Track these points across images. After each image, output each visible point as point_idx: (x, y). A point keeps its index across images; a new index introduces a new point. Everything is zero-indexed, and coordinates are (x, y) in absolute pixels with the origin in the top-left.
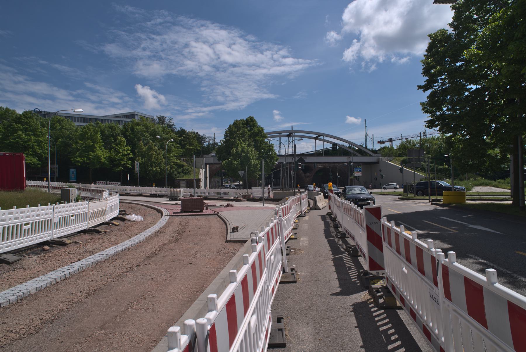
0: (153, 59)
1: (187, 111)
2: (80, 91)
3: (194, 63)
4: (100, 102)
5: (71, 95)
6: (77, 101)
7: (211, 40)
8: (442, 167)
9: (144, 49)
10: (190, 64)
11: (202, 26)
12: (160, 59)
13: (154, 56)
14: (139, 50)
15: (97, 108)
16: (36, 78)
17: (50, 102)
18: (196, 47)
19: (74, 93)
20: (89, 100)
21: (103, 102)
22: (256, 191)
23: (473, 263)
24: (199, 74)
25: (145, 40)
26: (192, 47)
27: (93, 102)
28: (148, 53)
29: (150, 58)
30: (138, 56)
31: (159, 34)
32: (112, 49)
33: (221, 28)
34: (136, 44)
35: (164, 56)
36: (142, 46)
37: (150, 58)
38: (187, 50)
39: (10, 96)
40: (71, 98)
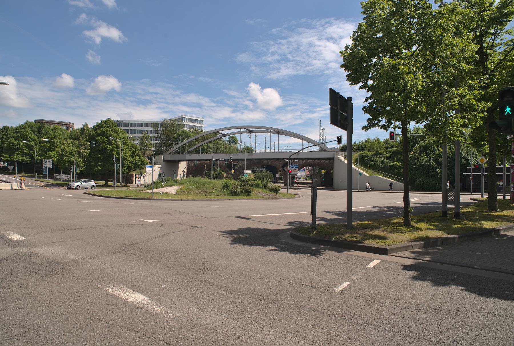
0: (282, 62)
1: (315, 110)
2: (218, 98)
3: (320, 62)
4: (236, 106)
5: (213, 102)
6: (217, 106)
7: (335, 36)
8: (471, 181)
9: (273, 54)
10: (317, 64)
11: (327, 23)
12: (287, 60)
13: (283, 60)
14: (269, 55)
15: (233, 112)
16: (187, 91)
17: (199, 109)
18: (320, 46)
19: (215, 100)
20: (226, 105)
21: (238, 106)
22: (213, 197)
23: (462, 290)
24: (325, 72)
25: (273, 45)
26: (315, 46)
27: (230, 106)
28: (276, 57)
29: (278, 61)
30: (268, 61)
31: (285, 38)
32: (243, 58)
33: (347, 21)
34: (265, 50)
35: (291, 58)
36: (270, 51)
37: (278, 61)
38: (312, 49)
39: (171, 106)
40: (213, 104)
